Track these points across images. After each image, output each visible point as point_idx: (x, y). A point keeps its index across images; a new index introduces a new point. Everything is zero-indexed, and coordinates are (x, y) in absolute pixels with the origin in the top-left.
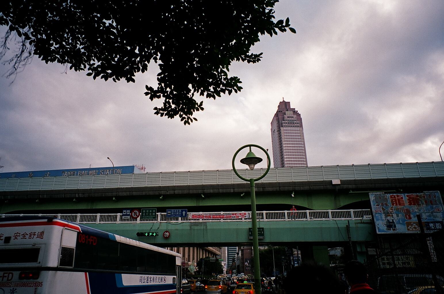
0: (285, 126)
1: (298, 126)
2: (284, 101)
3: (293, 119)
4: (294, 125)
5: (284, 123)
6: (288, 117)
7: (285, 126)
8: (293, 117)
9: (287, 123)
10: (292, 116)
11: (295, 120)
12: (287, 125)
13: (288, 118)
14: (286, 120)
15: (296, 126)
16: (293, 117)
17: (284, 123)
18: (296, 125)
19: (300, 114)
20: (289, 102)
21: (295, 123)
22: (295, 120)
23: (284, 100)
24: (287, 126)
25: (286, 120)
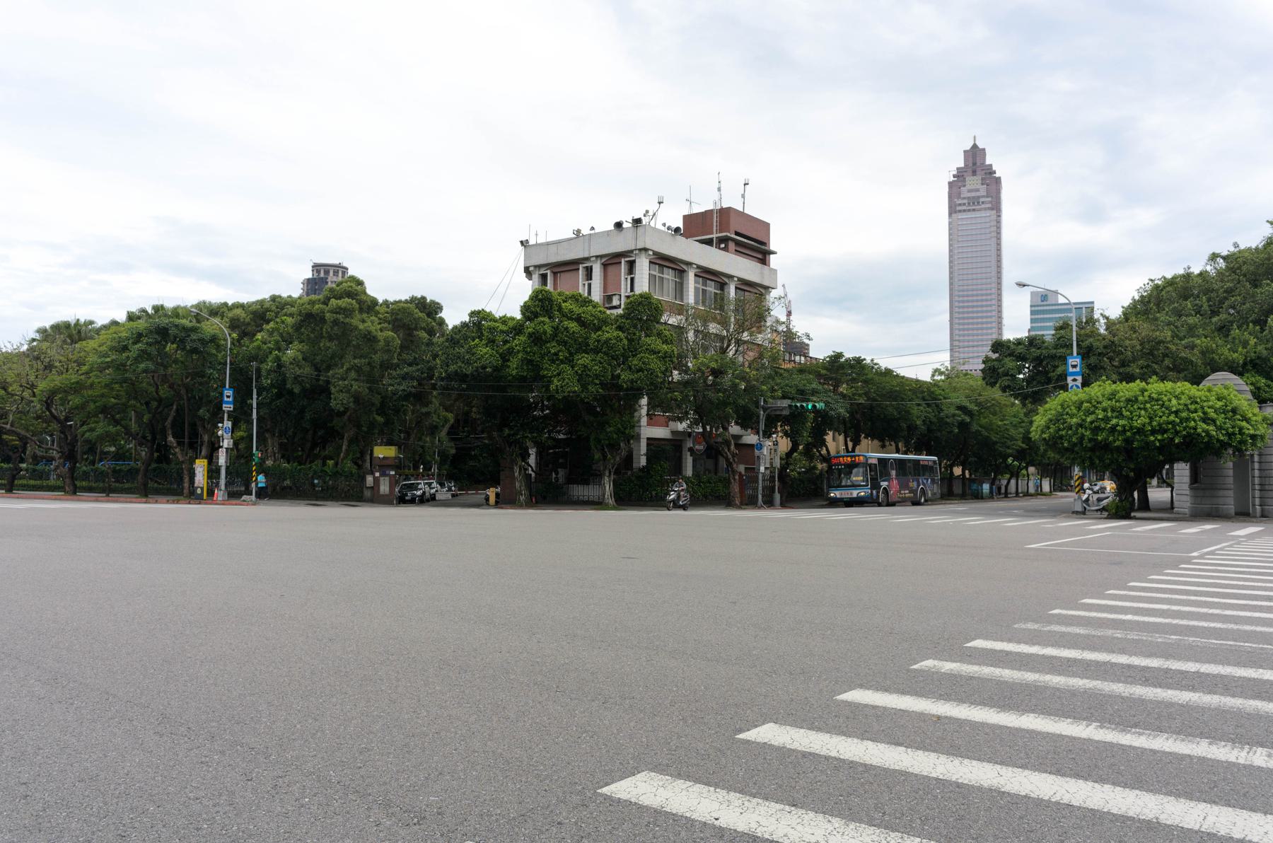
0: (960, 211)
2: (975, 146)
3: (978, 194)
5: (960, 205)
6: (969, 191)
7: (960, 211)
8: (978, 190)
9: (964, 204)
10: (978, 187)
11: (983, 197)
12: (964, 208)
14: (964, 198)
15: (985, 209)
17: (960, 205)
18: (983, 206)
19: (998, 180)
20: (984, 150)
21: (983, 203)
22: (983, 197)
23: (977, 143)
24: (964, 211)
25: (964, 198)
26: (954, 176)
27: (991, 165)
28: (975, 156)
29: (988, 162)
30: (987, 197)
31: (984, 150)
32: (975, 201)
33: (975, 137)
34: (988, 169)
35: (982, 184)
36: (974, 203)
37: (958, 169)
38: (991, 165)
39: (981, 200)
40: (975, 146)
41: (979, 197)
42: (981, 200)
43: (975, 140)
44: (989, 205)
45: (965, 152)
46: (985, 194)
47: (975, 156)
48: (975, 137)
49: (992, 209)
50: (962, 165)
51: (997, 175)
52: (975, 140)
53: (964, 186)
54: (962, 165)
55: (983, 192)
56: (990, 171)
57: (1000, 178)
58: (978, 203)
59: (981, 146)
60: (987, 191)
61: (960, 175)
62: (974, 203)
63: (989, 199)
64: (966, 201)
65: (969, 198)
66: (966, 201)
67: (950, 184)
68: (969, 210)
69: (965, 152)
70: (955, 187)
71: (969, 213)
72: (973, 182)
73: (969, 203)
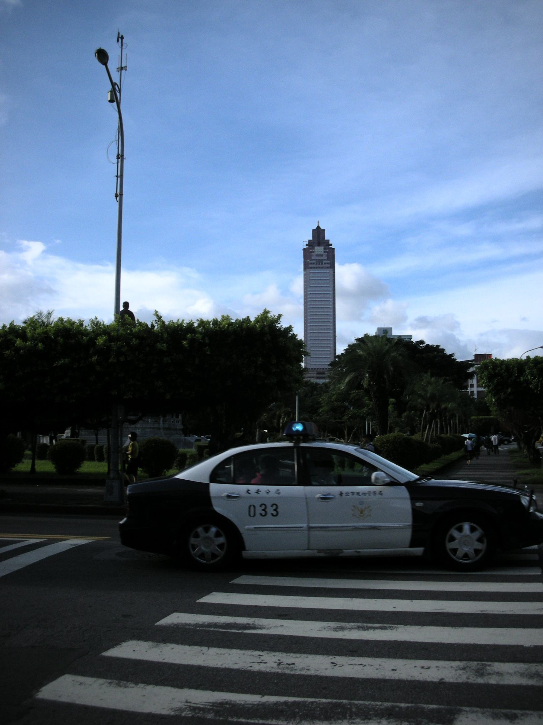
0: (311, 268)
1: (328, 268)
2: (318, 227)
3: (322, 258)
4: (323, 266)
5: (311, 264)
6: (317, 255)
8: (322, 256)
9: (314, 263)
11: (325, 260)
13: (317, 257)
14: (314, 260)
16: (322, 256)
17: (311, 264)
19: (334, 249)
20: (324, 230)
21: (325, 263)
22: (325, 260)
23: (320, 226)
24: (314, 268)
25: (314, 260)
26: (307, 245)
27: (329, 240)
28: (318, 233)
29: (326, 239)
30: (328, 260)
31: (324, 230)
32: (320, 262)
33: (318, 222)
34: (327, 243)
35: (325, 252)
36: (319, 264)
37: (309, 241)
38: (329, 240)
39: (324, 262)
40: (318, 227)
41: (322, 260)
42: (324, 262)
43: (318, 224)
44: (329, 266)
45: (313, 230)
46: (326, 258)
47: (318, 233)
48: (318, 222)
49: (330, 268)
50: (311, 239)
51: (332, 247)
52: (318, 224)
53: (314, 252)
54: (311, 239)
55: (325, 257)
56: (327, 244)
57: (334, 249)
58: (322, 264)
59: (322, 228)
60: (328, 256)
61: (311, 244)
62: (319, 264)
63: (329, 262)
64: (314, 262)
65: (316, 260)
66: (314, 262)
67: (304, 250)
68: (317, 268)
69: (313, 230)
70: (308, 252)
71: (317, 269)
72: (319, 250)
73: (317, 263)
